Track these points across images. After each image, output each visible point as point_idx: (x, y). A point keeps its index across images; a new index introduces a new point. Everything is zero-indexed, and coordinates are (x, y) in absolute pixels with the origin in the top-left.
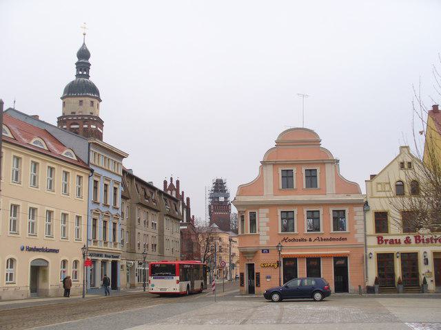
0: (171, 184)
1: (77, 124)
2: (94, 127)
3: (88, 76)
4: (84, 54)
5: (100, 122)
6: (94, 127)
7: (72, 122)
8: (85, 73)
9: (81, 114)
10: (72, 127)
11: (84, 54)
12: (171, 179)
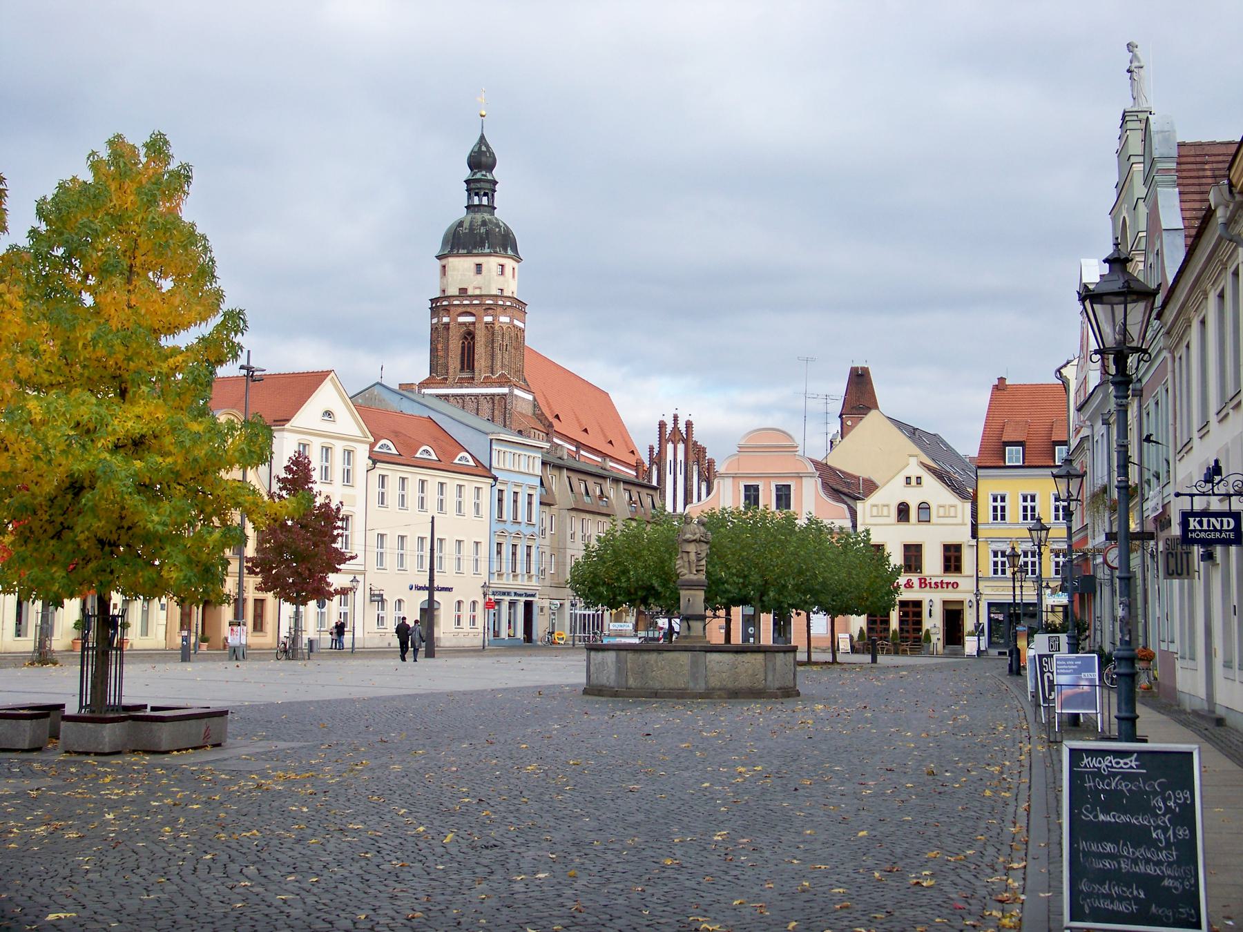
1: (472, 314)
2: (507, 320)
4: (481, 160)
6: (507, 320)
7: (461, 310)
8: (485, 201)
9: (477, 292)
10: (461, 319)
11: (481, 160)
12: (676, 418)
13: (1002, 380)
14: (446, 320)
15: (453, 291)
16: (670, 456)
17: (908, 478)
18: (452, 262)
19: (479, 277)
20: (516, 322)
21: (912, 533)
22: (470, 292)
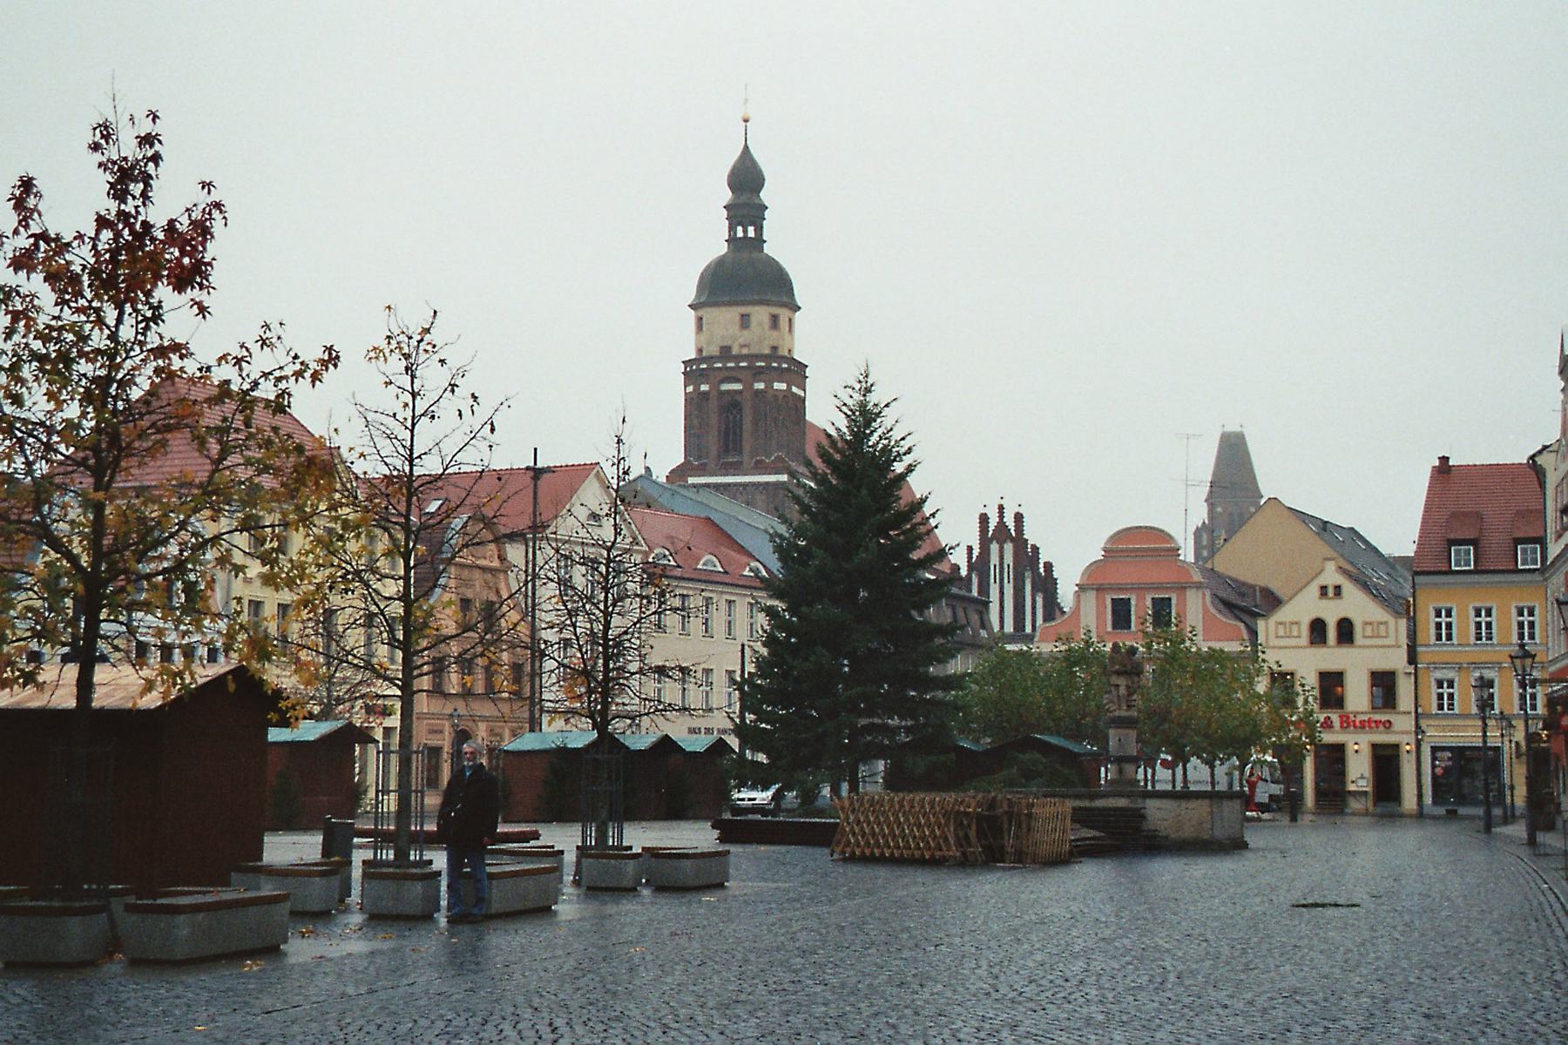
0: (1001, 524)
1: (737, 381)
2: (783, 386)
3: (759, 240)
4: (746, 181)
5: (797, 371)
6: (783, 386)
9: (745, 351)
10: (725, 387)
11: (746, 181)
12: (1001, 508)
13: (1444, 460)
14: (704, 388)
15: (714, 350)
16: (994, 560)
17: (1324, 589)
18: (709, 314)
19: (746, 332)
20: (794, 389)
21: (1332, 657)
22: (735, 351)
